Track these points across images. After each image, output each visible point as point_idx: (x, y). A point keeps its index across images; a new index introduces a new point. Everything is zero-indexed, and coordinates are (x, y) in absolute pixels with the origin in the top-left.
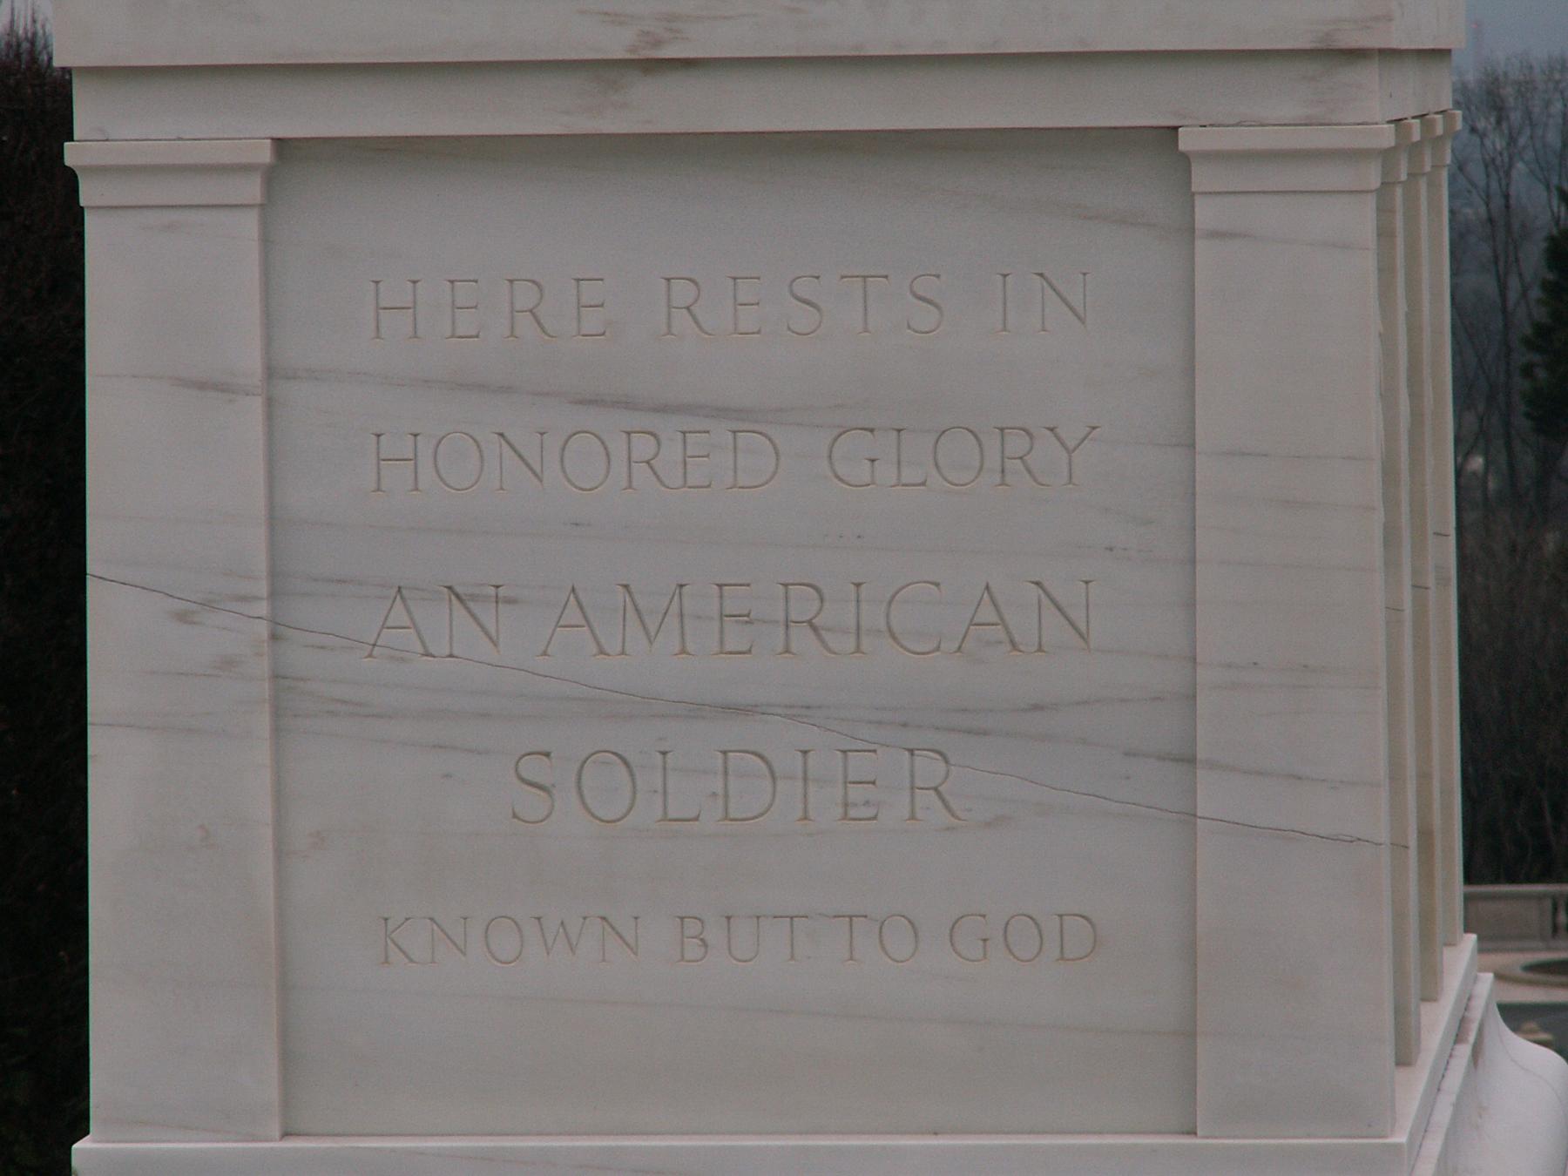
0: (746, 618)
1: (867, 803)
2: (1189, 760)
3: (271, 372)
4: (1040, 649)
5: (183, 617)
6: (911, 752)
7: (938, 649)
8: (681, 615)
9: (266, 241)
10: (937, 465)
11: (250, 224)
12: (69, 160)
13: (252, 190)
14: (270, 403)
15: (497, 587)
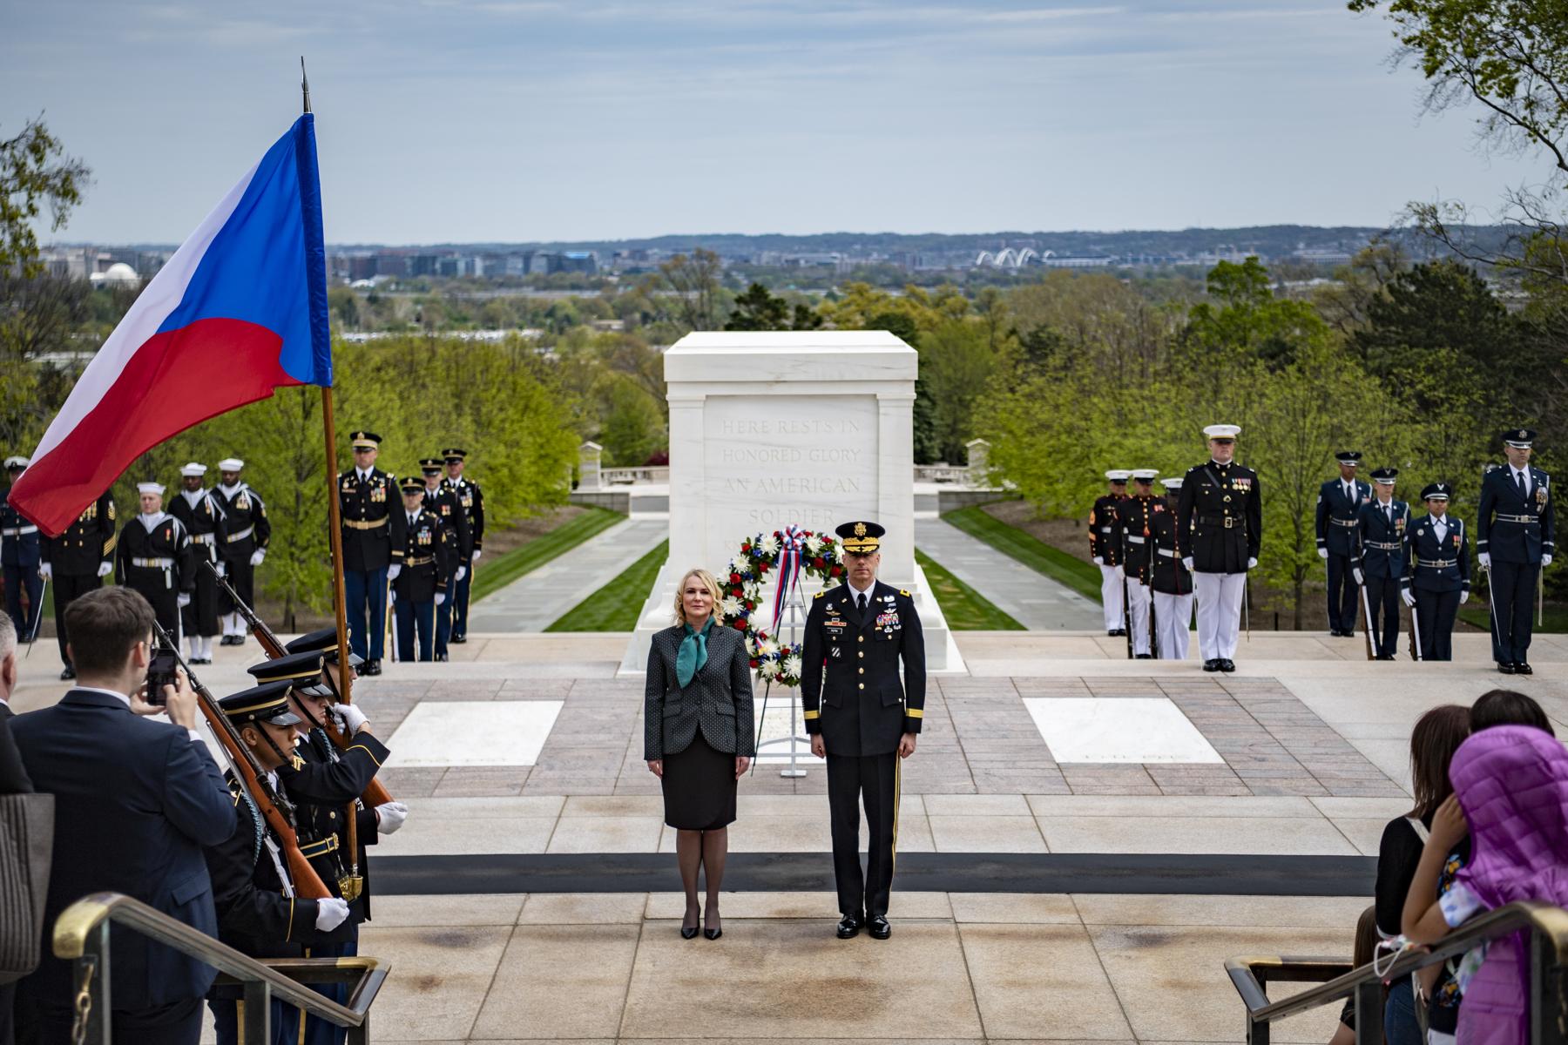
11: (701, 411)
13: (701, 404)
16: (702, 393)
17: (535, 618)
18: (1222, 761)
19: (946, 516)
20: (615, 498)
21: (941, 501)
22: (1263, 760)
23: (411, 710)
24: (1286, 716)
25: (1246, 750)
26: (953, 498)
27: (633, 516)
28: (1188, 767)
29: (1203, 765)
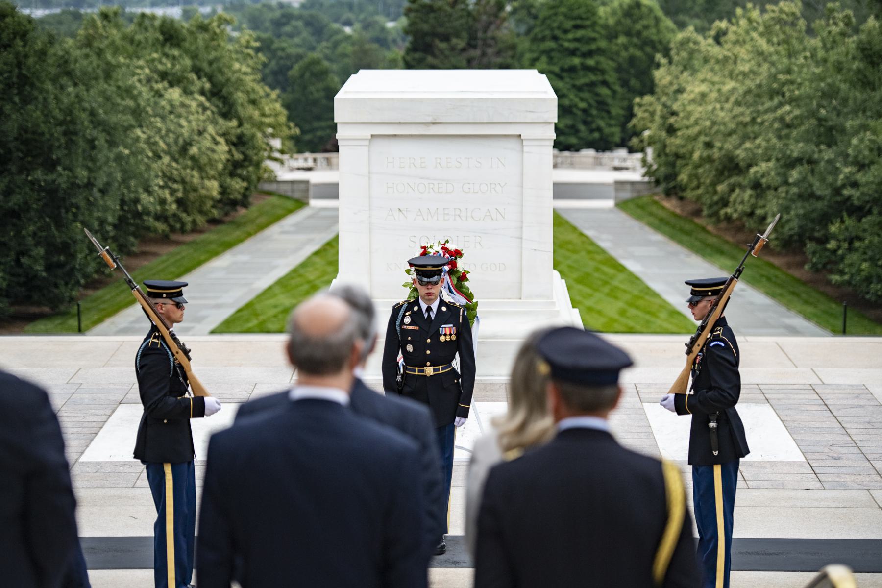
0: (448, 214)
1: (468, 245)
2: (521, 238)
3: (369, 173)
4: (497, 220)
5: (355, 213)
6: (475, 236)
7: (480, 219)
8: (437, 214)
9: (369, 151)
10: (480, 189)
11: (367, 148)
12: (337, 138)
13: (367, 143)
14: (370, 178)
15: (407, 209)
16: (367, 132)
17: (218, 306)
18: (803, 459)
19: (622, 205)
20: (296, 186)
21: (617, 190)
22: (839, 459)
23: (113, 411)
24: (867, 419)
25: (826, 450)
26: (628, 187)
27: (314, 203)
28: (774, 464)
29: (788, 462)
